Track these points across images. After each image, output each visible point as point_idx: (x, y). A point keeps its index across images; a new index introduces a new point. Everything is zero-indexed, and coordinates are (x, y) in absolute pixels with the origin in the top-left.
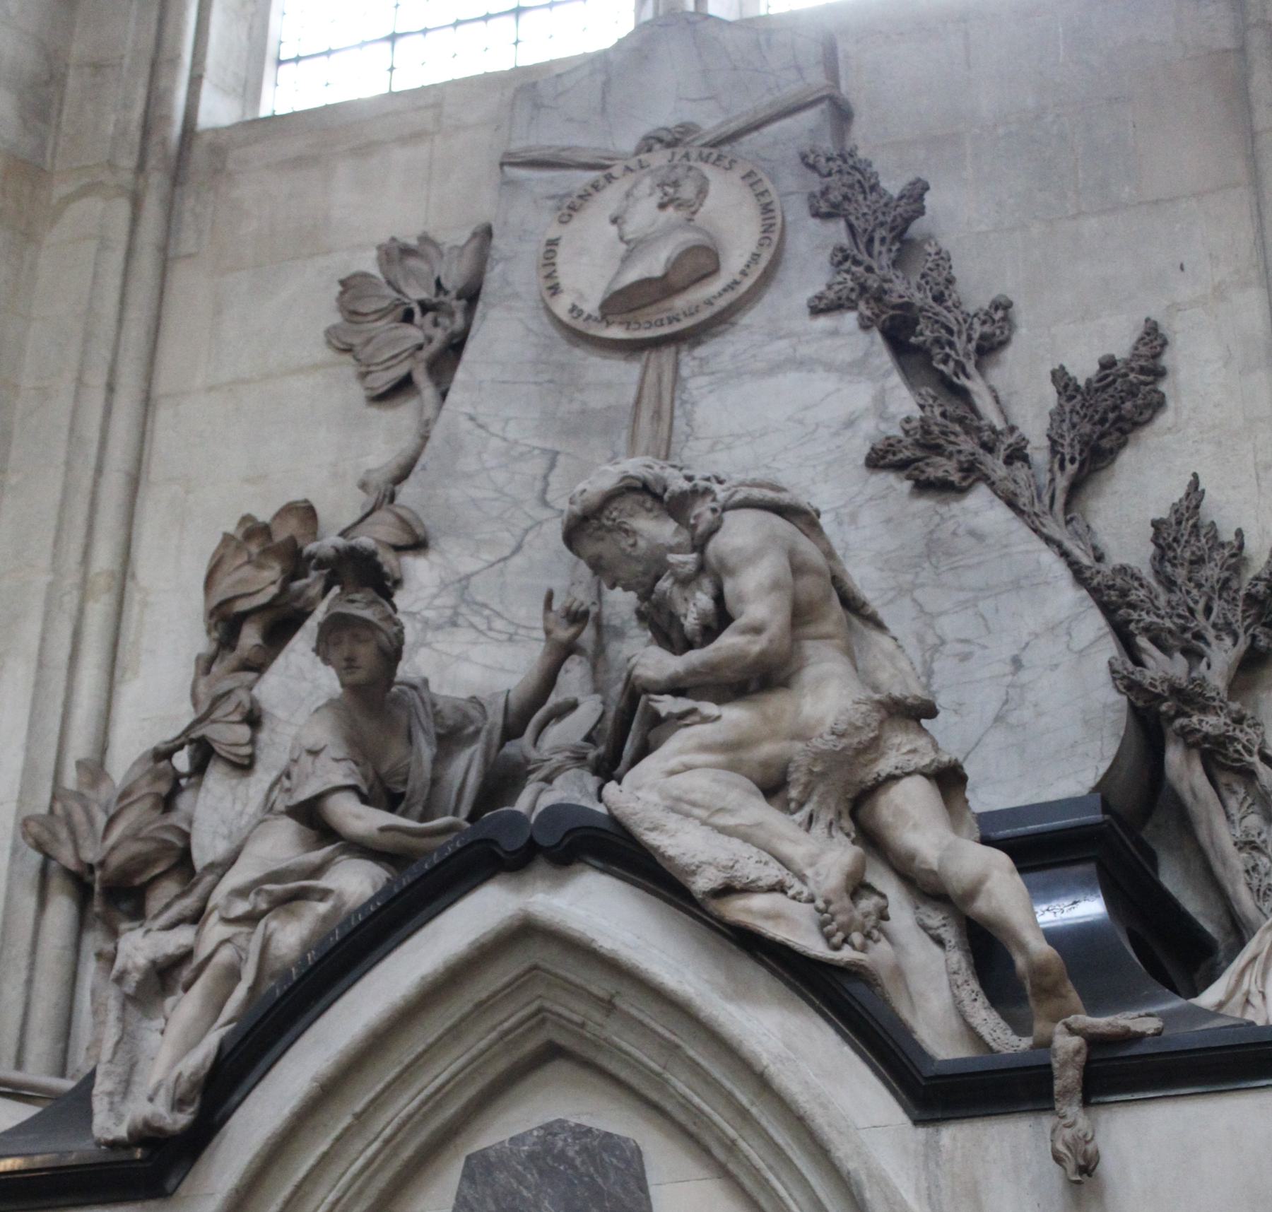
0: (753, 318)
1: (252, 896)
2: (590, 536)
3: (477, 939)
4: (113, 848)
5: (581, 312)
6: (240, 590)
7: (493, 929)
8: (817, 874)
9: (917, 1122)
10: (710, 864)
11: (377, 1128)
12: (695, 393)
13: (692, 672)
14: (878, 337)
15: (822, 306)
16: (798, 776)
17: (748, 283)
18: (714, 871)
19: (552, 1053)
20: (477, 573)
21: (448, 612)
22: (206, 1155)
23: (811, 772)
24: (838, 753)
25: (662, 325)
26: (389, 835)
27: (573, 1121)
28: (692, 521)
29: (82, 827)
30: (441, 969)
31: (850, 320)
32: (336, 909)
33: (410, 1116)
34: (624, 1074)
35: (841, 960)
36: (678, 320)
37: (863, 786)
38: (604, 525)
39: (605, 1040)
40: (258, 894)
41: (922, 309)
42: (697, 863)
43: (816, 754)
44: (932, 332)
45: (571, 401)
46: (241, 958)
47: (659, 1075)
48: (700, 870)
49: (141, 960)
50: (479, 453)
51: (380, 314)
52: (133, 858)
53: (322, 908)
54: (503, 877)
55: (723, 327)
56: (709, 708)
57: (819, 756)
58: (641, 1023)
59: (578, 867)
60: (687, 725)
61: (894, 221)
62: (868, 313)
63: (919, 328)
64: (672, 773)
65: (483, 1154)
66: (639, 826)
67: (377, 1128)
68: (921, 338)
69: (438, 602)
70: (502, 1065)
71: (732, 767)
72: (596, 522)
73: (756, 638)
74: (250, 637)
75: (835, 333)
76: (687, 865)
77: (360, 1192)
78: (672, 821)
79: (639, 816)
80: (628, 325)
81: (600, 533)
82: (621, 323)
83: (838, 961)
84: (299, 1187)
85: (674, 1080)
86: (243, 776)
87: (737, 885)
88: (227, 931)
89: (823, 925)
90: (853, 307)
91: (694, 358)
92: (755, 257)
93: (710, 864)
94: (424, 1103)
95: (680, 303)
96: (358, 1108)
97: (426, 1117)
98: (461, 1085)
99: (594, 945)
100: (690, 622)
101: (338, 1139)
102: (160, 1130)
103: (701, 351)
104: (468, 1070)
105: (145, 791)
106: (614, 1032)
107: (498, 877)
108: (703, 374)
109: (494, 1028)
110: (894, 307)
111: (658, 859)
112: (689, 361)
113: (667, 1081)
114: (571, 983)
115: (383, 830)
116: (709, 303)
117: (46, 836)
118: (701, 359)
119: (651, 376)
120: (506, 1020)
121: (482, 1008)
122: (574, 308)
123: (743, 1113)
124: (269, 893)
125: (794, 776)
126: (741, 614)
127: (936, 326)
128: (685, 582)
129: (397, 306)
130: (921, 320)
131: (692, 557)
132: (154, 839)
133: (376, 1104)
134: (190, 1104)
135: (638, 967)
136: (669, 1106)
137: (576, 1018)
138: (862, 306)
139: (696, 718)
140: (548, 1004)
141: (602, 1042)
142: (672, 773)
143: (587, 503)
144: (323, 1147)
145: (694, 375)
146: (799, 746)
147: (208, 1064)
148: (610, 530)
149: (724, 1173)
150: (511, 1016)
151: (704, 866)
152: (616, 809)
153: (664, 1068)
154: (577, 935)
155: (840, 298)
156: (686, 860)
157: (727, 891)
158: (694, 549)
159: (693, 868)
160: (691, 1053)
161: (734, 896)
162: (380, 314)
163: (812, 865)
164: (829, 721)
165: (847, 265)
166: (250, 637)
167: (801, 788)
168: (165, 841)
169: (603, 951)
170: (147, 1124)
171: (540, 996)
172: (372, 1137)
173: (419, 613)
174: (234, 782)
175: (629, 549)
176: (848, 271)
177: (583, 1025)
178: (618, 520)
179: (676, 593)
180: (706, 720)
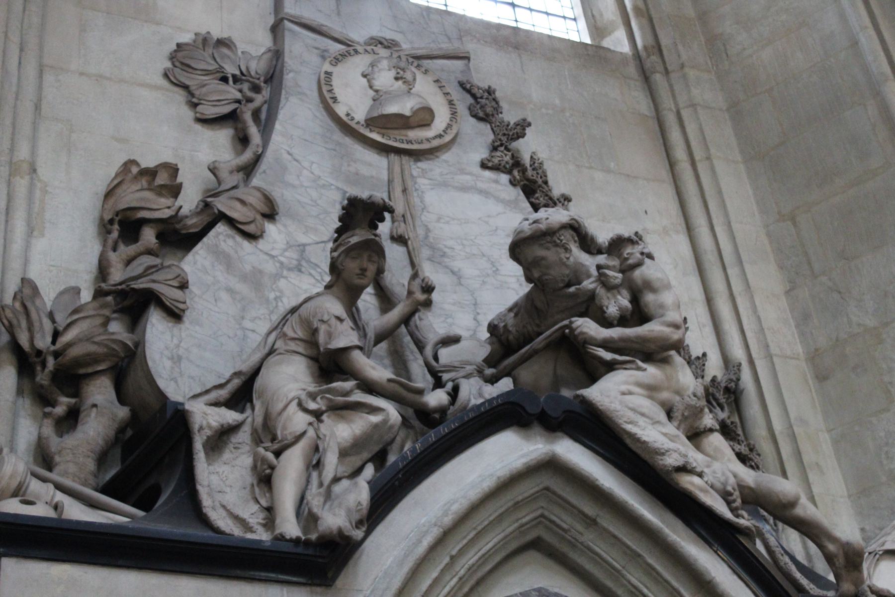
0: (446, 156)
1: (318, 399)
2: (541, 245)
3: (528, 462)
4: (69, 345)
5: (353, 119)
6: (143, 205)
7: (536, 458)
8: (714, 472)
10: (676, 451)
12: (423, 187)
13: (623, 340)
14: (521, 193)
15: (490, 164)
16: (677, 414)
17: (447, 138)
18: (678, 455)
19: (536, 545)
20: (309, 245)
21: (295, 262)
22: (351, 563)
23: (683, 415)
24: (696, 408)
25: (403, 143)
26: (392, 384)
28: (626, 256)
29: (36, 324)
30: (508, 476)
31: (504, 178)
32: (385, 421)
33: (473, 565)
34: (589, 567)
35: (742, 525)
36: (412, 143)
37: (698, 430)
38: (555, 242)
39: (582, 543)
40: (321, 398)
41: (540, 186)
42: (666, 449)
43: (688, 405)
44: (544, 199)
45: (349, 165)
46: (318, 437)
48: (669, 453)
49: (214, 424)
50: (298, 176)
51: (206, 72)
52: (89, 355)
53: (375, 419)
54: (515, 428)
55: (431, 157)
56: (640, 363)
57: (689, 407)
58: (615, 537)
59: (560, 434)
60: (626, 369)
61: (513, 135)
62: (518, 177)
63: (537, 195)
64: (623, 394)
66: (620, 419)
68: (537, 201)
69: (287, 254)
70: (514, 545)
71: (650, 397)
72: (550, 238)
73: (676, 331)
74: (149, 236)
75: (496, 182)
76: (658, 449)
78: (642, 421)
79: (619, 413)
80: (383, 135)
81: (550, 245)
82: (378, 133)
83: (741, 525)
85: (629, 576)
86: (176, 322)
87: (689, 467)
88: (310, 418)
89: (729, 503)
90: (509, 172)
91: (418, 168)
92: (449, 126)
93: (676, 451)
94: (480, 559)
95: (412, 134)
96: (454, 553)
98: (496, 552)
99: (597, 483)
100: (612, 310)
103: (420, 164)
104: (501, 543)
105: (91, 313)
106: (589, 538)
107: (513, 428)
108: (425, 178)
109: (517, 520)
110: (528, 180)
111: (628, 441)
112: (416, 168)
113: (623, 576)
114: (569, 503)
115: (390, 380)
116: (428, 140)
117: (15, 322)
118: (423, 170)
119: (397, 169)
120: (524, 517)
121: (517, 506)
122: (348, 115)
124: (330, 400)
125: (676, 414)
126: (662, 316)
127: (546, 198)
128: (610, 287)
129: (218, 72)
130: (538, 191)
131: (620, 275)
132: (106, 346)
133: (462, 552)
135: (627, 502)
137: (565, 526)
138: (516, 173)
139: (634, 366)
140: (546, 513)
141: (578, 544)
142: (623, 394)
143: (551, 226)
144: (435, 574)
145: (419, 177)
146: (678, 398)
148: (557, 245)
150: (526, 516)
151: (671, 452)
152: (602, 406)
153: (623, 568)
154: (587, 474)
155: (500, 165)
156: (657, 445)
157: (684, 469)
158: (622, 271)
159: (663, 451)
160: (651, 561)
161: (684, 474)
162: (206, 72)
163: (708, 466)
164: (691, 390)
165: (502, 148)
166: (149, 236)
167: (678, 422)
168: (114, 349)
169: (604, 487)
170: (340, 531)
171: (542, 507)
172: (454, 574)
173: (277, 257)
174: (170, 325)
175: (565, 260)
176: (502, 152)
178: (564, 242)
179: (601, 291)
180: (639, 369)
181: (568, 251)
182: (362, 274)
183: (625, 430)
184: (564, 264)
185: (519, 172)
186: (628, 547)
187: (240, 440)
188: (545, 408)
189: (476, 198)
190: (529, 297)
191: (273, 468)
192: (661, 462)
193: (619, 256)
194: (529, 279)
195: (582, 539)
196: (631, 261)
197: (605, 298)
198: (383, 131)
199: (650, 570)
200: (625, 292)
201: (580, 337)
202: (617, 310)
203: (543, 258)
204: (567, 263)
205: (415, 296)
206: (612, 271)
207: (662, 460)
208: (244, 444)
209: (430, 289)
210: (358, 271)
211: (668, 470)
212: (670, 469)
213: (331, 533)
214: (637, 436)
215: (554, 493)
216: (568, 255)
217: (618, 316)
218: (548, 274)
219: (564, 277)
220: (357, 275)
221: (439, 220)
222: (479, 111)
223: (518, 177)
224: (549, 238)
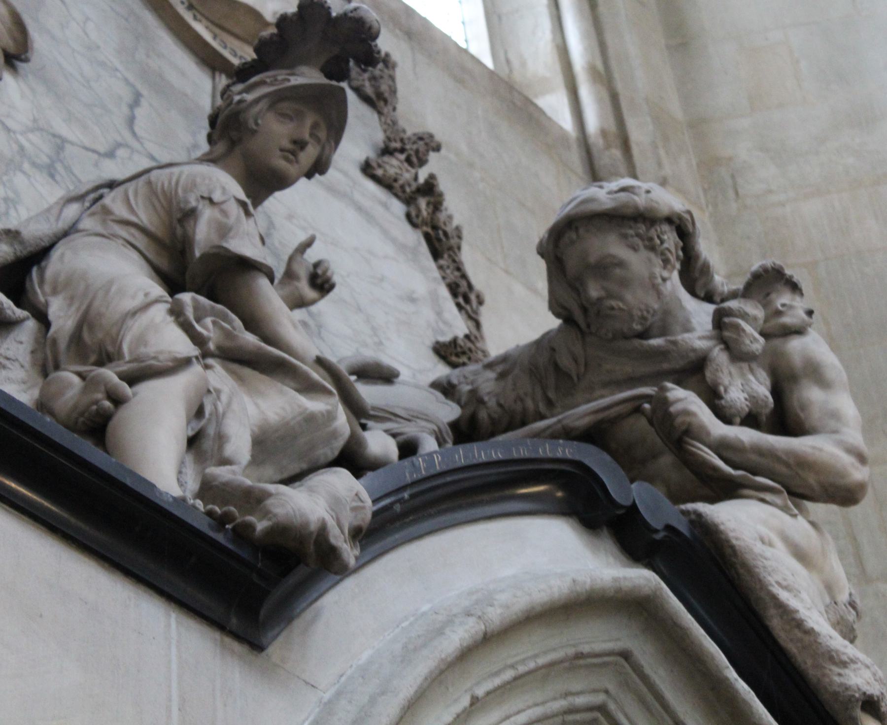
2: (625, 236)
13: (759, 451)
20: (72, 143)
21: (46, 160)
38: (651, 239)
60: (763, 501)
62: (424, 213)
66: (770, 575)
72: (644, 228)
75: (385, 206)
76: (837, 651)
90: (409, 201)
107: (571, 520)
111: (775, 624)
124: (228, 335)
130: (446, 256)
138: (422, 202)
140: (612, 707)
143: (655, 205)
148: (652, 248)
151: (859, 665)
152: (737, 539)
155: (396, 180)
159: (845, 658)
165: (402, 157)
171: (607, 692)
173: (14, 132)
181: (669, 267)
182: (293, 153)
183: (774, 598)
184: (656, 288)
185: (428, 204)
187: (10, 354)
188: (637, 502)
189: (351, 215)
190: (544, 344)
191: (118, 401)
192: (837, 679)
193: (766, 304)
194: (556, 307)
196: (787, 320)
197: (726, 371)
198: (217, 31)
200: (763, 375)
201: (679, 420)
202: (746, 399)
203: (621, 264)
204: (662, 288)
205: (296, 283)
206: (751, 325)
207: (840, 675)
208: (17, 364)
209: (327, 286)
210: (286, 144)
211: (853, 696)
212: (857, 695)
213: (306, 524)
214: (798, 616)
215: (638, 669)
216: (665, 274)
217: (747, 409)
218: (621, 299)
219: (648, 312)
220: (282, 150)
221: (290, 217)
222: (367, 84)
223: (424, 213)
224: (642, 228)
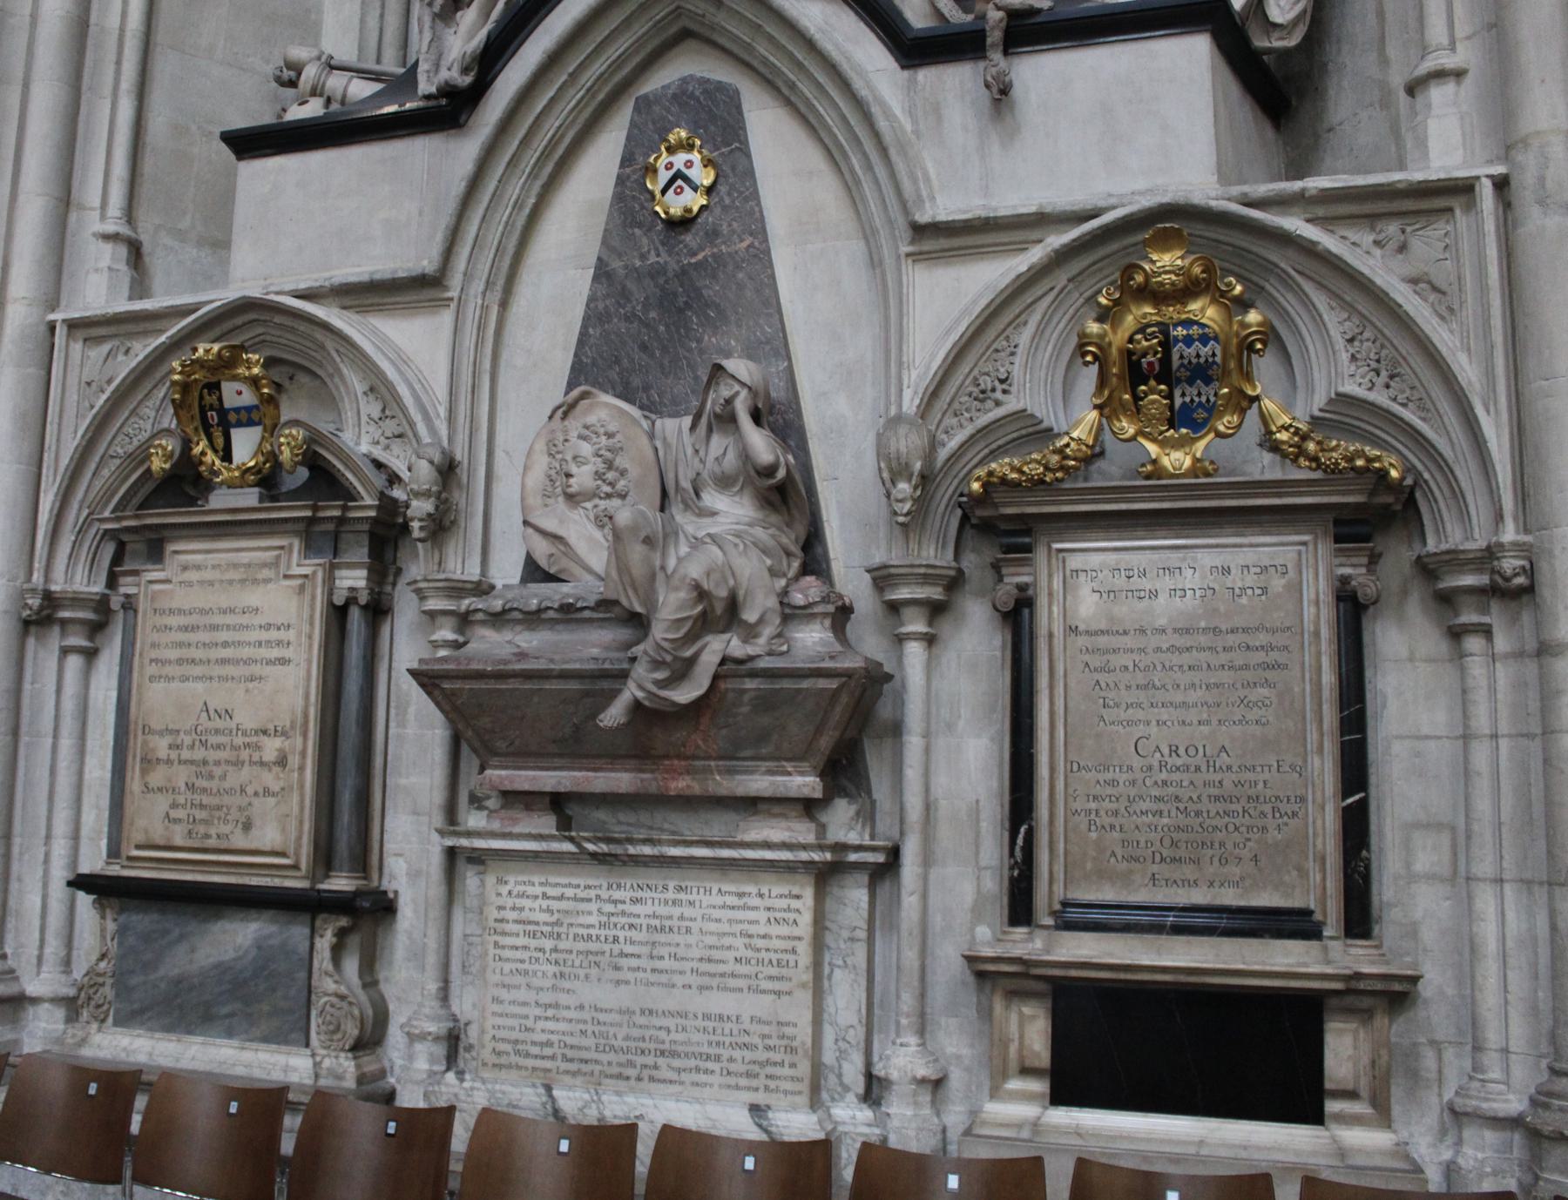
9: (903, 67)
11: (582, 82)
19: (685, 35)
22: (484, 100)
27: (699, 75)
33: (602, 74)
34: (728, 45)
47: (749, 44)
65: (646, 97)
67: (582, 82)
70: (655, 42)
77: (573, 121)
84: (538, 118)
85: (758, 47)
94: (609, 66)
96: (571, 70)
97: (612, 74)
101: (560, 89)
102: (455, 87)
113: (754, 48)
123: (800, 66)
133: (582, 67)
134: (472, 70)
136: (755, 63)
137: (700, 12)
144: (551, 94)
147: (482, 46)
149: (788, 103)
160: (768, 29)
177: (703, 16)
186: (751, 20)
195: (716, 20)
199: (771, 39)
